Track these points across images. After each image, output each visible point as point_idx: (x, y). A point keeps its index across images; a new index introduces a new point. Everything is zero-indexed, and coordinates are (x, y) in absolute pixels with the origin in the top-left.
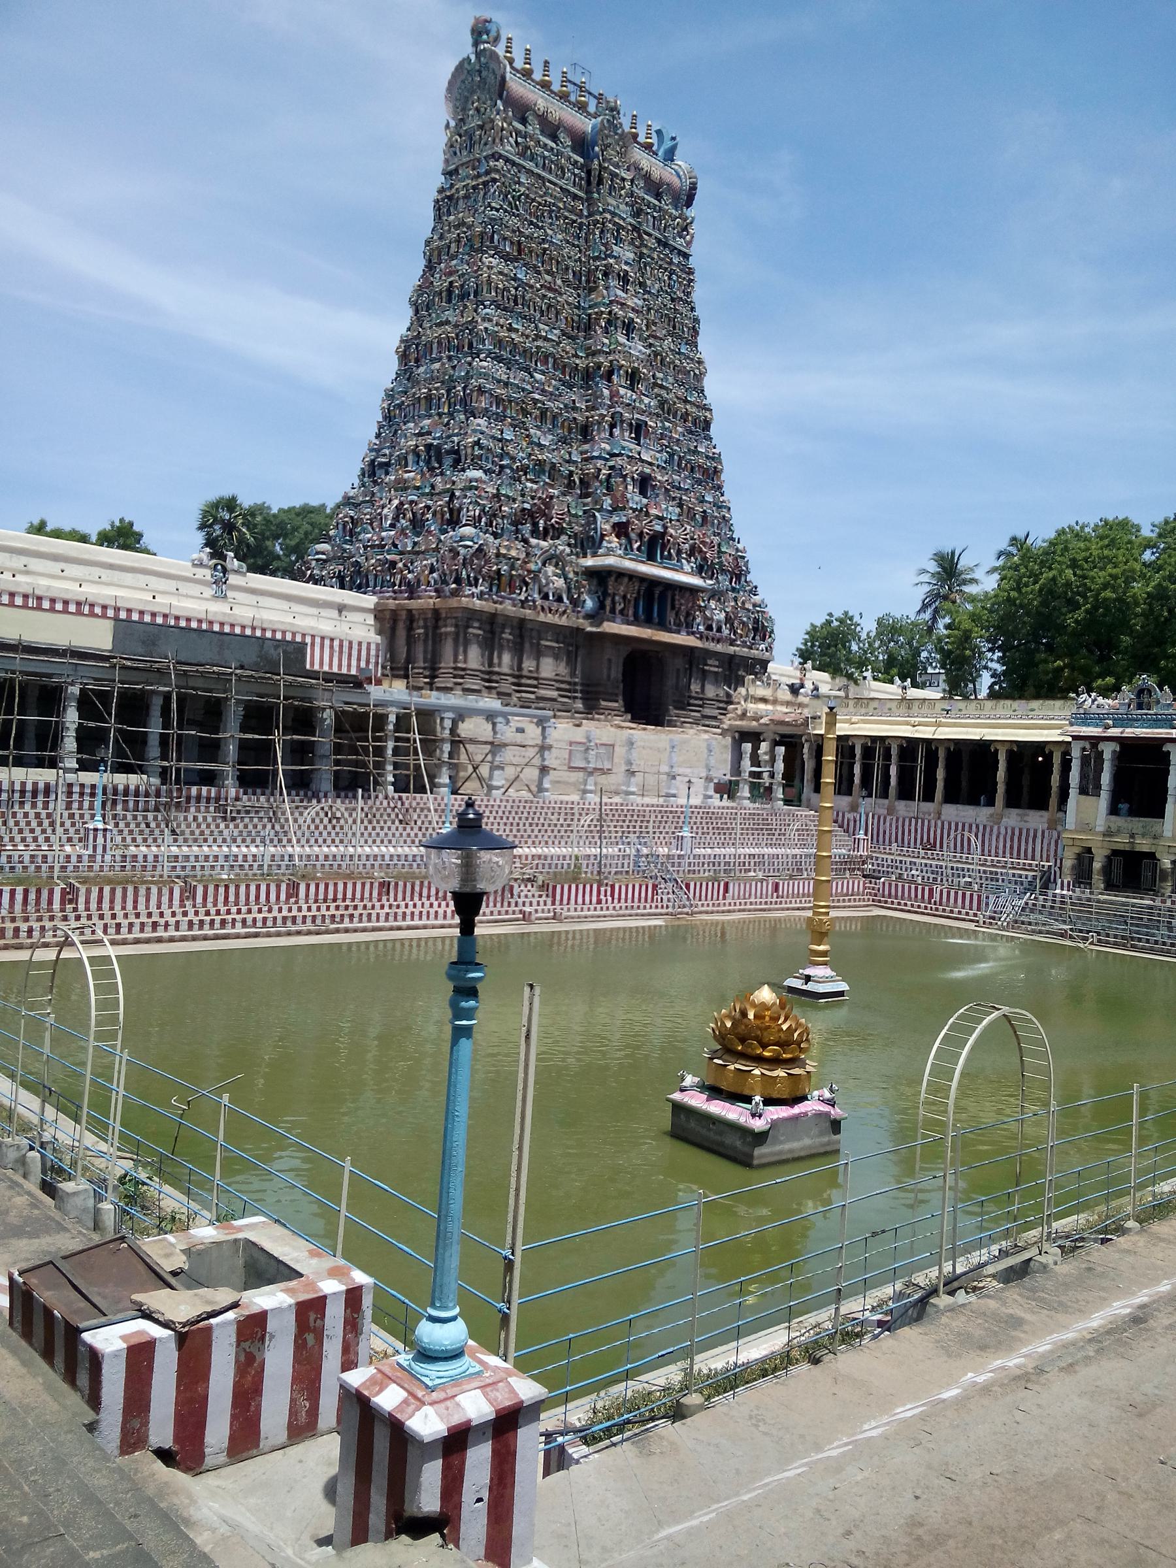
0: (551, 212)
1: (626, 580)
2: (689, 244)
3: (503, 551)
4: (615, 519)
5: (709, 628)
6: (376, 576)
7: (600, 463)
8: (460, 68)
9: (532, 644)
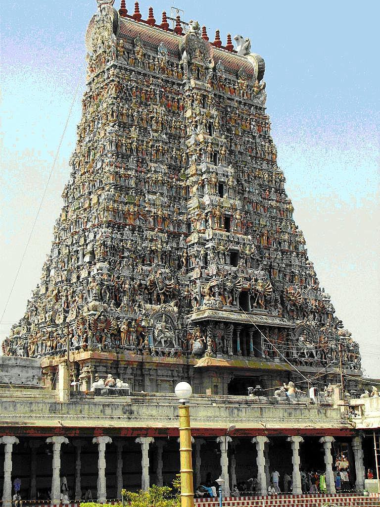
2: (263, 103)
6: (42, 344)
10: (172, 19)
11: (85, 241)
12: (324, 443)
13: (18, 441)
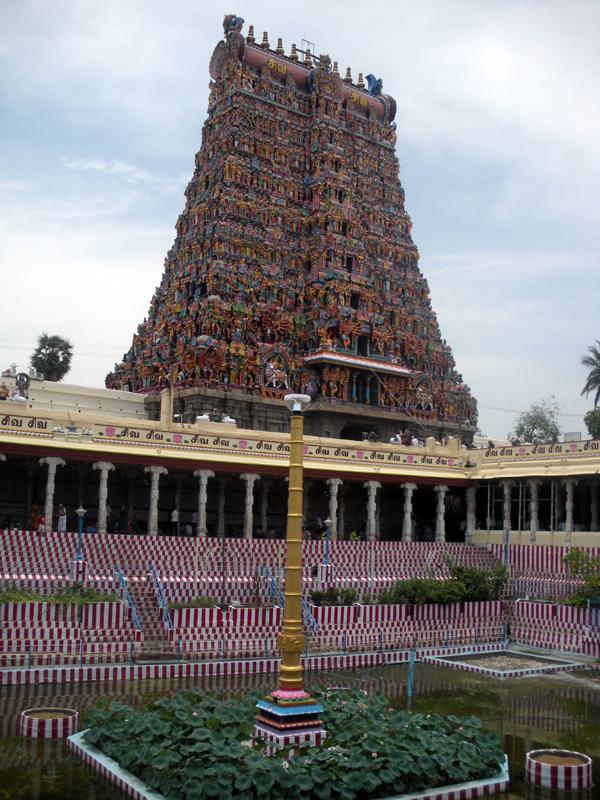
0: (280, 125)
1: (338, 369)
2: (394, 143)
3: (233, 351)
4: (328, 325)
5: (420, 407)
7: (316, 286)
8: (218, 48)
9: (259, 422)
10: (303, 52)
11: (197, 273)
12: (439, 492)
13: (114, 468)
